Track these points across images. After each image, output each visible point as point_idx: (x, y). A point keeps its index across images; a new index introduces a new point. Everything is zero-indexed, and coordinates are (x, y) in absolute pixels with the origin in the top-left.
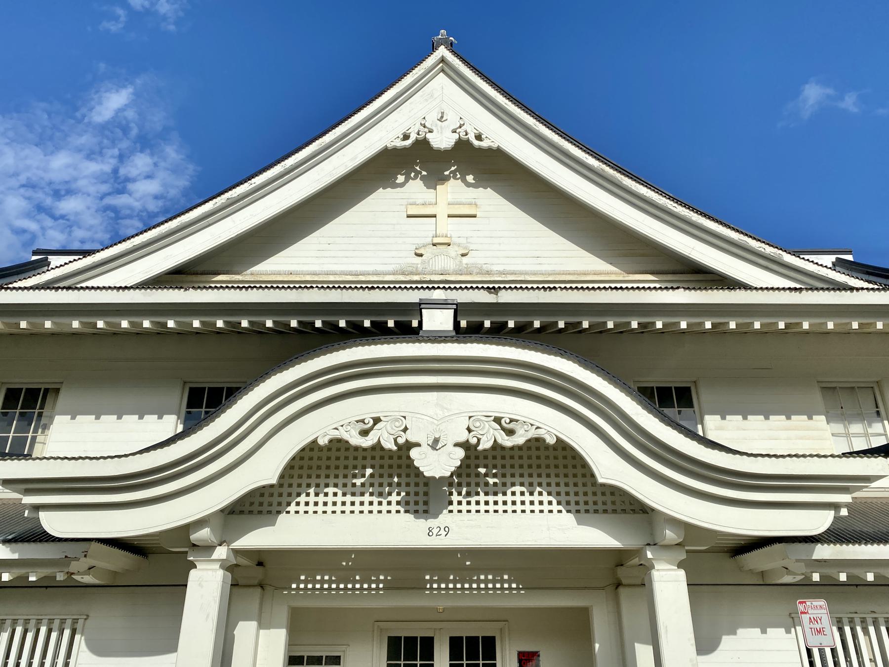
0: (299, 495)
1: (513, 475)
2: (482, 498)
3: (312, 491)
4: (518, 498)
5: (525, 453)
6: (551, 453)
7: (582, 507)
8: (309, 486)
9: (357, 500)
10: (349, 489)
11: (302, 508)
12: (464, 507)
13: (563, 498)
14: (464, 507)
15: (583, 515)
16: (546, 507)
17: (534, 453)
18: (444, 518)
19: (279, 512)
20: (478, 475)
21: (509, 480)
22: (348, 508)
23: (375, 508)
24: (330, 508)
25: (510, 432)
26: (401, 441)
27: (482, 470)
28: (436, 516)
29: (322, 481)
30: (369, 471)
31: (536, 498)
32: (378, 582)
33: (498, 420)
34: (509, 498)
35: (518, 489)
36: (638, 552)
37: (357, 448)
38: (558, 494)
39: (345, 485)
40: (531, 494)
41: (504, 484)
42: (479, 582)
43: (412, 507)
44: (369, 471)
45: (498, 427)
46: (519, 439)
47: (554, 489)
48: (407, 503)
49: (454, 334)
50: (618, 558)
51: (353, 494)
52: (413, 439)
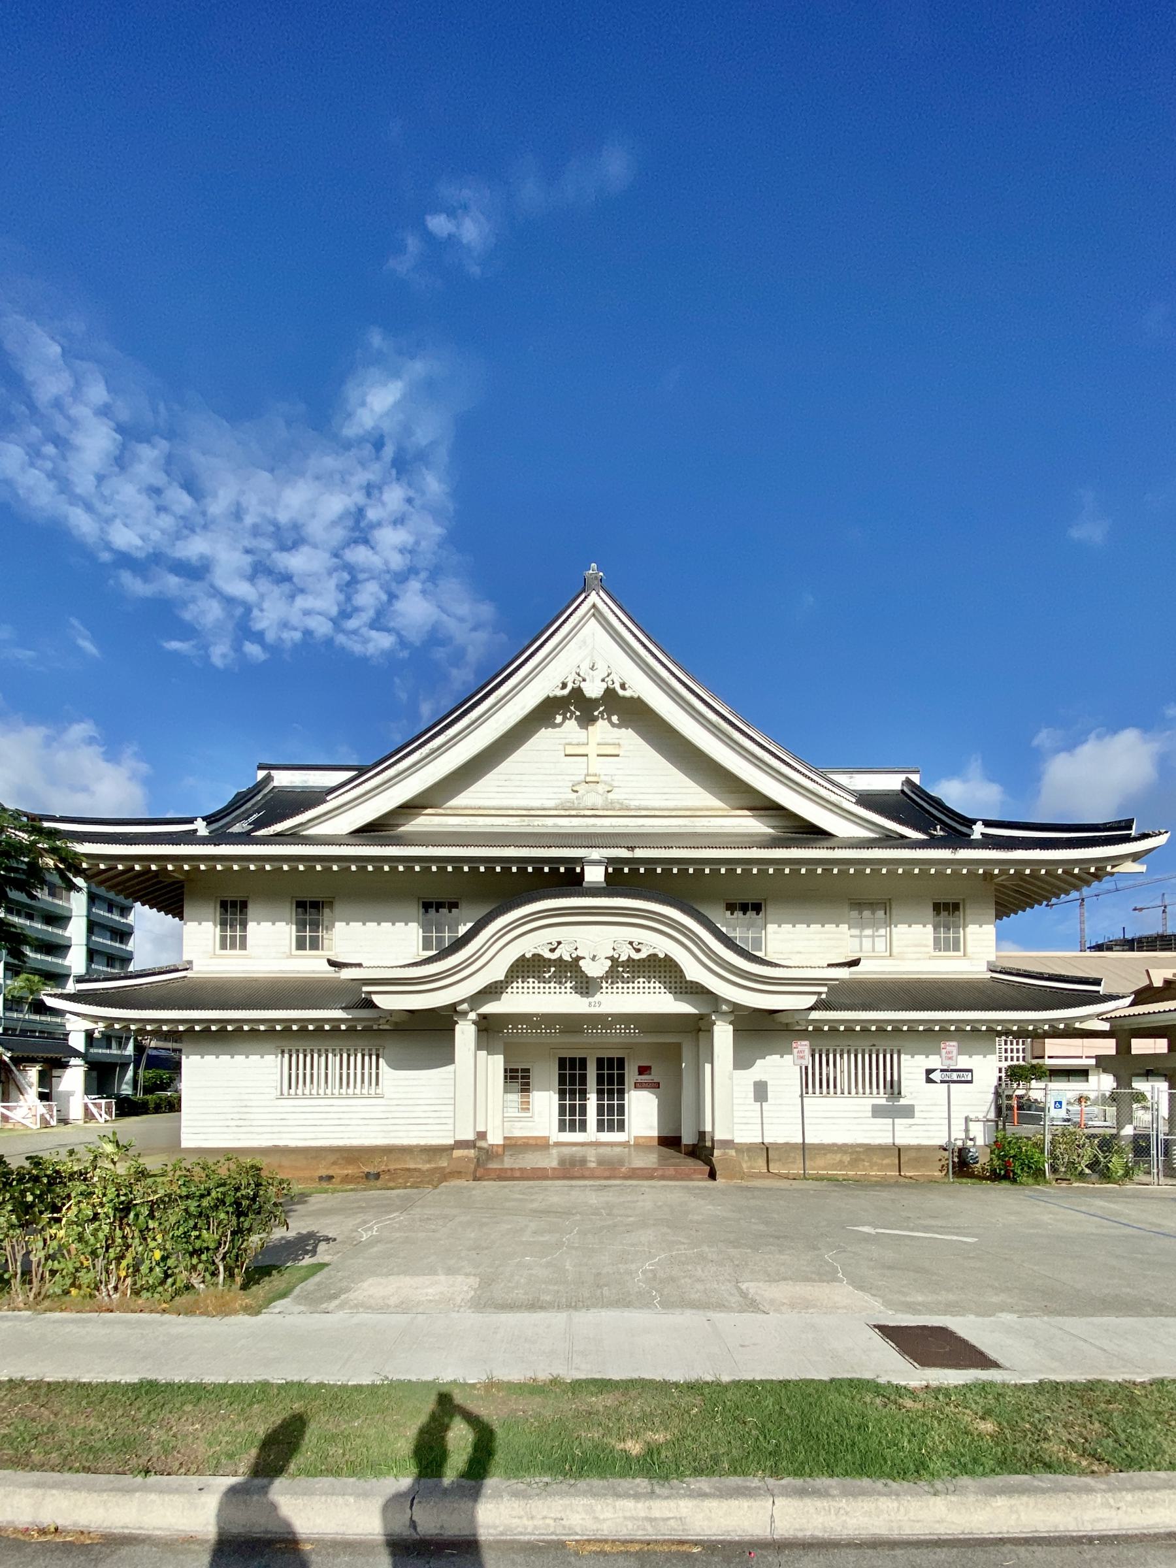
0: (512, 982)
1: (639, 972)
2: (620, 985)
3: (520, 980)
4: (641, 985)
7: (678, 990)
8: (518, 977)
9: (547, 986)
10: (542, 979)
11: (515, 990)
12: (610, 990)
13: (668, 985)
14: (610, 990)
15: (679, 996)
16: (657, 990)
18: (598, 997)
19: (502, 993)
21: (636, 975)
22: (542, 990)
23: (558, 990)
24: (531, 990)
25: (638, 951)
26: (574, 956)
27: (620, 969)
28: (593, 996)
29: (526, 974)
30: (553, 969)
31: (652, 985)
33: (631, 943)
34: (636, 985)
35: (641, 980)
36: (709, 1015)
37: (550, 960)
38: (665, 982)
39: (539, 977)
40: (649, 982)
41: (634, 977)
43: (579, 990)
44: (553, 969)
45: (630, 946)
46: (643, 955)
47: (662, 980)
48: (576, 988)
49: (605, 885)
51: (544, 982)
52: (581, 955)
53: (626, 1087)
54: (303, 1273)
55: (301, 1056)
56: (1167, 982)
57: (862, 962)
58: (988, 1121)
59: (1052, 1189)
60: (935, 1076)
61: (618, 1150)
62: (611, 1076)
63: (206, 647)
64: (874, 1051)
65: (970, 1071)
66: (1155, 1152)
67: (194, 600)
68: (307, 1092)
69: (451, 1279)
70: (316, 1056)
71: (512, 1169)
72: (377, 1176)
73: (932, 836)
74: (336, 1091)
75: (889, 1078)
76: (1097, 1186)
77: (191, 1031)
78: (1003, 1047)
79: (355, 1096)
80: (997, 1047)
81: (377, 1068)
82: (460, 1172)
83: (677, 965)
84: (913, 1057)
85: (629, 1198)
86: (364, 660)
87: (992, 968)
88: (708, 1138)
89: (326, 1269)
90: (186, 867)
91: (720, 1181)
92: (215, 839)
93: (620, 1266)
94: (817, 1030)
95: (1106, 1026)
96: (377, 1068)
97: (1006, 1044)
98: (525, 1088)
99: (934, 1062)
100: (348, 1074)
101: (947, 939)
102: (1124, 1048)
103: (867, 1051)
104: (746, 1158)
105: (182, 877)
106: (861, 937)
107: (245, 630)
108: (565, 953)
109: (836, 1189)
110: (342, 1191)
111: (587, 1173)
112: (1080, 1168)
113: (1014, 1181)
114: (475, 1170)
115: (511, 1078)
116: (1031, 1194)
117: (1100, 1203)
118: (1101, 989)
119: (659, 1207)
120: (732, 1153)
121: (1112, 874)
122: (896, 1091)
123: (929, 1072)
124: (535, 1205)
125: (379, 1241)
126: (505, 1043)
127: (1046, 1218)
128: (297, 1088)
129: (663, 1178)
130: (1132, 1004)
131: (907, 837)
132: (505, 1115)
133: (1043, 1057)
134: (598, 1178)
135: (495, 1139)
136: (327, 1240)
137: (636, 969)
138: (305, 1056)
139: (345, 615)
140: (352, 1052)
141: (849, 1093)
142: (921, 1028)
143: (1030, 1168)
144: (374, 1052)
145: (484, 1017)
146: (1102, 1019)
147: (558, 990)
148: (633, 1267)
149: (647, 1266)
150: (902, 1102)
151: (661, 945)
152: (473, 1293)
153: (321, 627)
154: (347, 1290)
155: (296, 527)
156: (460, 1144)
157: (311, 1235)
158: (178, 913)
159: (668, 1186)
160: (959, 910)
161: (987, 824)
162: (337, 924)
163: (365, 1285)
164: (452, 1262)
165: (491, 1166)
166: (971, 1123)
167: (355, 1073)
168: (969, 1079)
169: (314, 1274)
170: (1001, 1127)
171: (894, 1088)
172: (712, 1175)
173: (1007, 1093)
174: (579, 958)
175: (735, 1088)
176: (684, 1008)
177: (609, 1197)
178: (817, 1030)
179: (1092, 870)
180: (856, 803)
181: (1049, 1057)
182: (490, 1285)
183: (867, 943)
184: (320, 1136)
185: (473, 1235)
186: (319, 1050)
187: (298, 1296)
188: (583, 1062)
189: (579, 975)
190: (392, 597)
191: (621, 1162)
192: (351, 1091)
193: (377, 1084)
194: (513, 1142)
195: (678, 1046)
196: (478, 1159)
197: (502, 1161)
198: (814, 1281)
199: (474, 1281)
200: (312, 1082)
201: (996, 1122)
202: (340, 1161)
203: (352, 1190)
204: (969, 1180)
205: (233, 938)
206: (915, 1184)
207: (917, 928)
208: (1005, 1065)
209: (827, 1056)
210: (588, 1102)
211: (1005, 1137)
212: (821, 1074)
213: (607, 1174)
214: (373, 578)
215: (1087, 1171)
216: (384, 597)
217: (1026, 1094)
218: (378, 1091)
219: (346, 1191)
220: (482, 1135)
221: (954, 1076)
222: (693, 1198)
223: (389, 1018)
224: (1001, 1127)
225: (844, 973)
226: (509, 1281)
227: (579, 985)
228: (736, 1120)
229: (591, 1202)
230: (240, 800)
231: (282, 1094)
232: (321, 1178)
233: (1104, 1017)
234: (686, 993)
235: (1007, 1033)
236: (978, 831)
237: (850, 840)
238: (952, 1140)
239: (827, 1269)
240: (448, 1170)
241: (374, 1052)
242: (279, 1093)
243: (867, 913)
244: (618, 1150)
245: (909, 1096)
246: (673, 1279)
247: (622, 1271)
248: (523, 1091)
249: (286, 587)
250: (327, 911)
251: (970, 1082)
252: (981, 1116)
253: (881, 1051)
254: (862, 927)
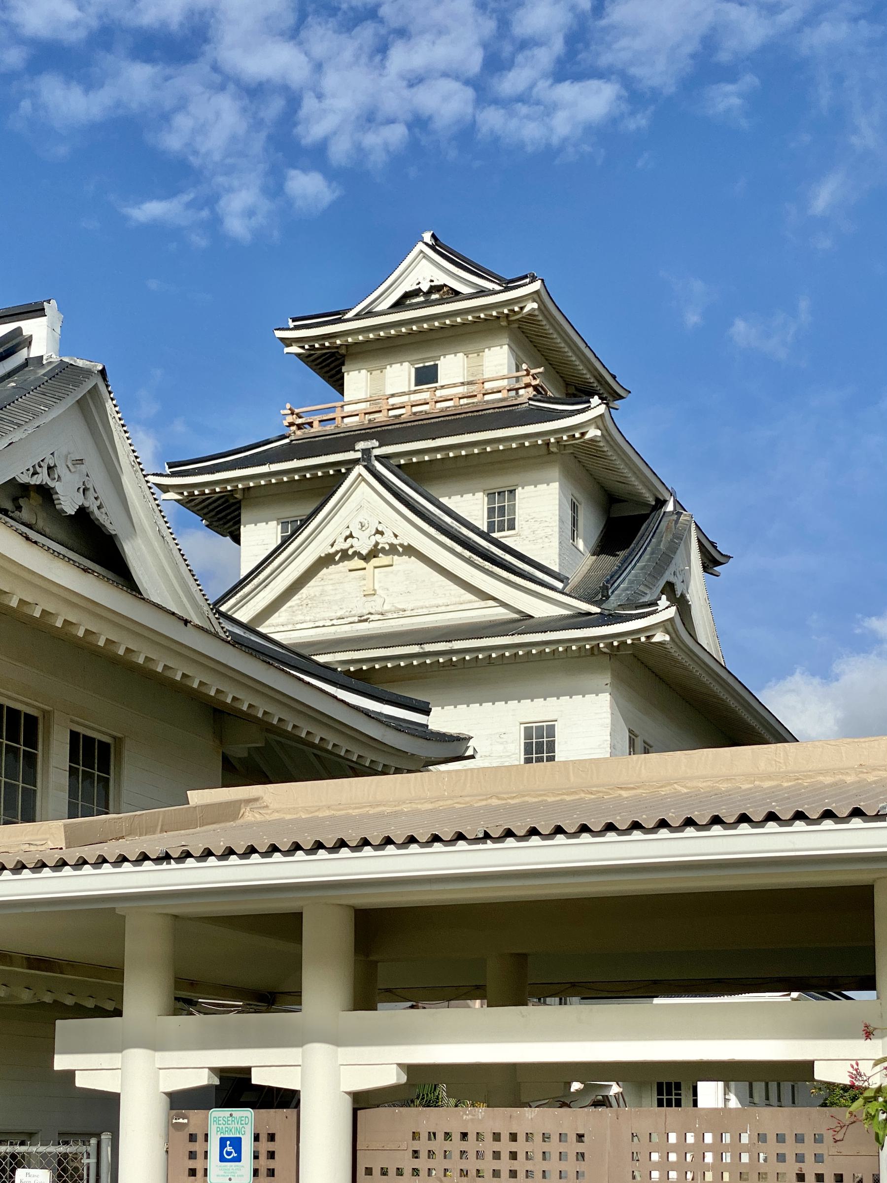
67: (182, 105)
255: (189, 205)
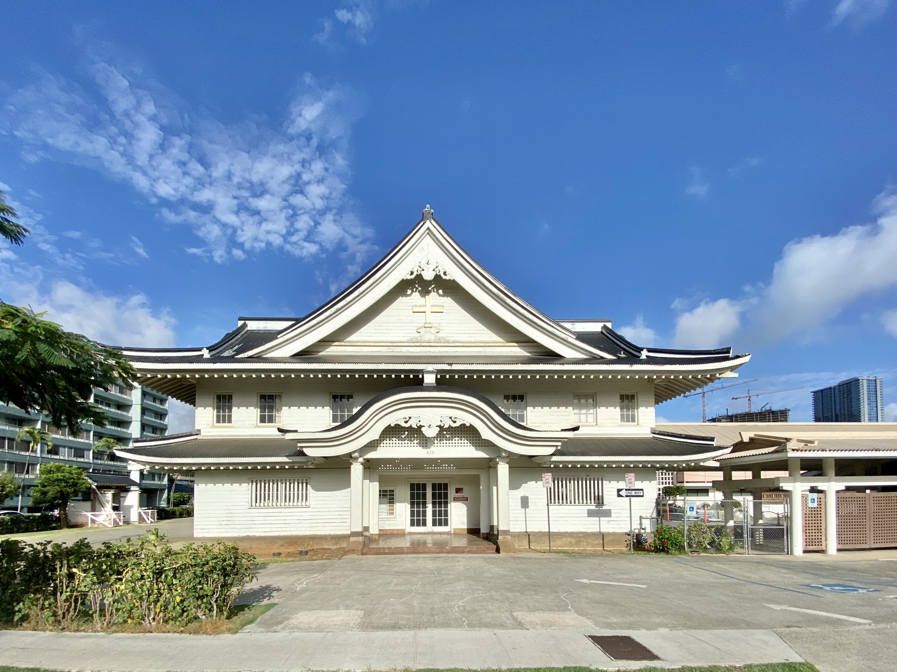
0: (383, 440)
2: (445, 441)
3: (388, 439)
4: (457, 442)
5: (459, 429)
6: (468, 429)
7: (478, 444)
8: (387, 437)
9: (403, 442)
11: (385, 445)
12: (439, 445)
13: (472, 442)
14: (439, 445)
16: (466, 444)
17: (463, 429)
18: (432, 448)
19: (377, 446)
20: (443, 434)
22: (400, 445)
23: (409, 445)
24: (394, 445)
25: (455, 422)
26: (418, 425)
29: (391, 436)
31: (463, 441)
32: (408, 467)
33: (450, 418)
34: (454, 442)
35: (457, 439)
36: (495, 459)
37: (405, 428)
42: (443, 467)
43: (421, 445)
44: (406, 433)
46: (457, 424)
47: (468, 438)
48: (420, 443)
50: (490, 460)
52: (422, 425)
53: (449, 500)
54: (262, 609)
55: (263, 484)
56: (751, 439)
57: (580, 428)
58: (652, 518)
59: (688, 557)
60: (623, 493)
61: (444, 536)
62: (440, 494)
63: (211, 251)
64: (588, 479)
65: (642, 490)
66: (746, 535)
68: (266, 504)
69: (348, 611)
70: (271, 484)
71: (384, 548)
72: (306, 553)
73: (619, 358)
74: (283, 504)
75: (596, 494)
76: (714, 555)
77: (199, 470)
78: (661, 476)
79: (294, 507)
80: (657, 476)
81: (306, 490)
82: (354, 550)
83: (477, 430)
84: (610, 482)
85: (450, 564)
86: (301, 259)
87: (654, 432)
88: (495, 529)
89: (276, 607)
90: (197, 376)
91: (502, 554)
92: (213, 360)
93: (444, 603)
94: (556, 467)
95: (717, 464)
96: (306, 490)
97: (662, 475)
98: (391, 501)
99: (622, 485)
100: (290, 494)
101: (628, 416)
102: (727, 477)
103: (584, 479)
104: (517, 540)
105: (194, 382)
106: (580, 414)
107: (233, 242)
108: (413, 423)
109: (568, 558)
110: (286, 562)
111: (427, 550)
112: (704, 545)
113: (668, 553)
114: (363, 549)
115: (383, 495)
116: (677, 560)
117: (716, 565)
118: (714, 443)
119: (467, 569)
120: (509, 537)
121: (719, 378)
122: (601, 502)
123: (619, 490)
124: (396, 569)
125: (306, 591)
126: (380, 476)
127: (685, 574)
128: (260, 502)
129: (470, 552)
130: (732, 452)
131: (604, 358)
132: (380, 517)
133: (683, 482)
134: (433, 553)
135: (374, 531)
136: (279, 590)
137: (454, 432)
138: (265, 484)
139: (290, 233)
140: (292, 481)
141: (575, 503)
142: (614, 466)
143: (676, 545)
144: (304, 481)
145: (368, 460)
146: (715, 460)
147: (409, 445)
148: (452, 604)
149: (460, 603)
150: (604, 508)
151: (468, 419)
152: (360, 620)
153: (277, 240)
154: (288, 619)
155: (262, 184)
156: (354, 534)
157: (267, 587)
158: (193, 402)
159: (473, 557)
160: (634, 399)
161: (649, 350)
162: (284, 408)
163: (298, 615)
164: (348, 602)
165: (371, 546)
166: (643, 520)
167: (294, 494)
168: (642, 494)
169: (268, 610)
170: (660, 522)
171: (599, 501)
172: (498, 551)
173: (663, 502)
174: (421, 427)
175: (510, 500)
176: (481, 454)
177: (439, 564)
178: (556, 467)
179: (708, 376)
180: (576, 339)
181: (687, 482)
182: (370, 615)
183: (583, 417)
184: (274, 529)
185: (360, 587)
186: (273, 481)
187: (260, 622)
188: (424, 486)
189: (421, 436)
190: (317, 223)
191: (446, 543)
192: (291, 504)
193: (306, 500)
194: (384, 532)
195: (478, 476)
196: (364, 543)
197: (378, 544)
198: (555, 611)
199: (361, 613)
200: (269, 499)
201: (657, 519)
202: (285, 544)
203: (292, 561)
204: (642, 552)
205: (224, 416)
206: (612, 554)
207: (611, 409)
208: (662, 486)
209: (562, 482)
210: (427, 509)
211: (662, 528)
212: (558, 492)
213: (438, 550)
214: (306, 213)
215: (708, 547)
216: (312, 223)
217: (674, 503)
218: (307, 504)
219: (289, 561)
220: (366, 529)
221: (633, 493)
222: (486, 564)
223: (313, 461)
224: (660, 522)
225: (570, 435)
226: (381, 613)
227: (421, 442)
228: (511, 519)
229: (429, 567)
230: (229, 337)
231: (252, 506)
232: (274, 554)
233: (716, 459)
234: (482, 446)
235: (662, 468)
236: (644, 354)
237: (572, 360)
238: (633, 529)
239: (562, 604)
240: (347, 549)
241: (304, 481)
242: (250, 505)
243: (583, 401)
244: (444, 536)
245: (607, 504)
246: (474, 611)
247: (446, 606)
248: (390, 503)
249: (257, 218)
250: (277, 400)
251: (642, 496)
252: (648, 516)
253: (592, 479)
254: (581, 409)
255: (204, 251)
